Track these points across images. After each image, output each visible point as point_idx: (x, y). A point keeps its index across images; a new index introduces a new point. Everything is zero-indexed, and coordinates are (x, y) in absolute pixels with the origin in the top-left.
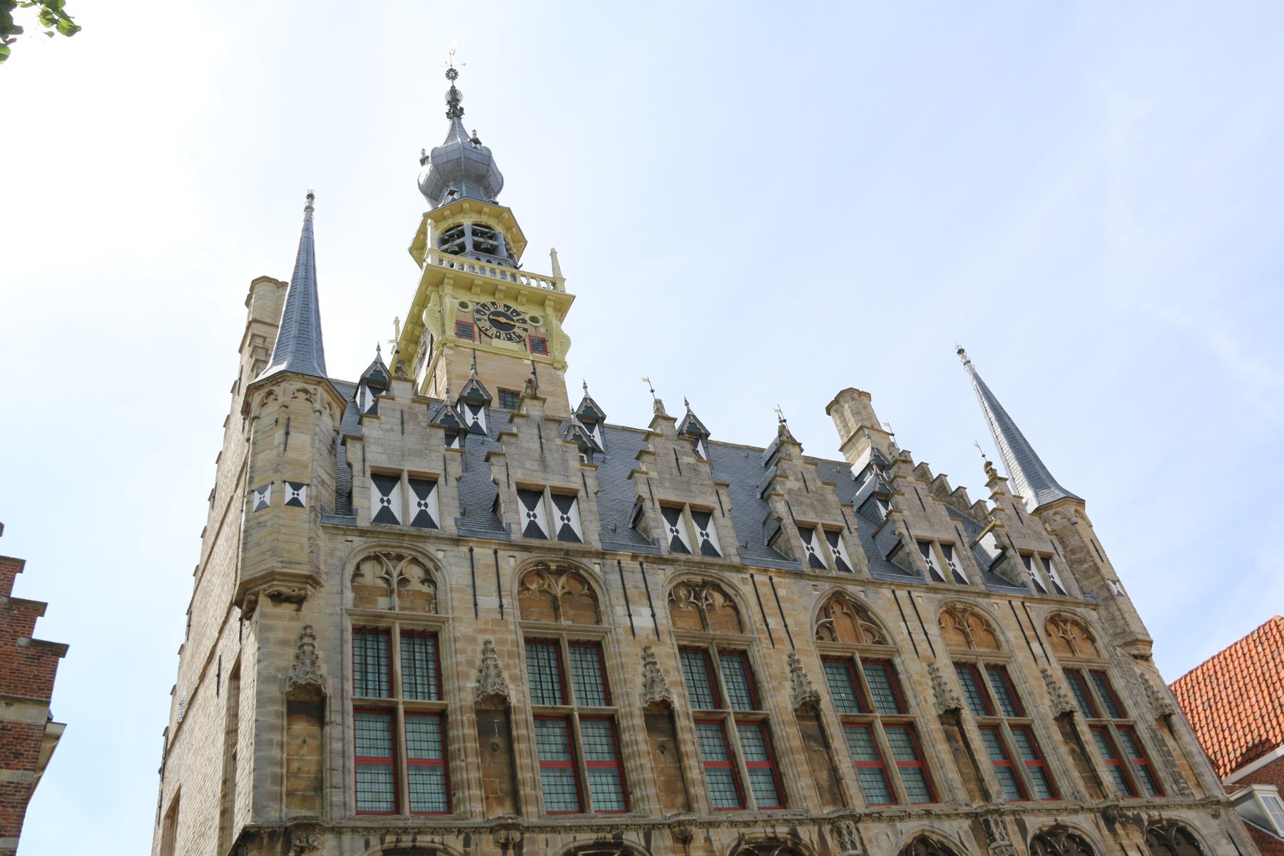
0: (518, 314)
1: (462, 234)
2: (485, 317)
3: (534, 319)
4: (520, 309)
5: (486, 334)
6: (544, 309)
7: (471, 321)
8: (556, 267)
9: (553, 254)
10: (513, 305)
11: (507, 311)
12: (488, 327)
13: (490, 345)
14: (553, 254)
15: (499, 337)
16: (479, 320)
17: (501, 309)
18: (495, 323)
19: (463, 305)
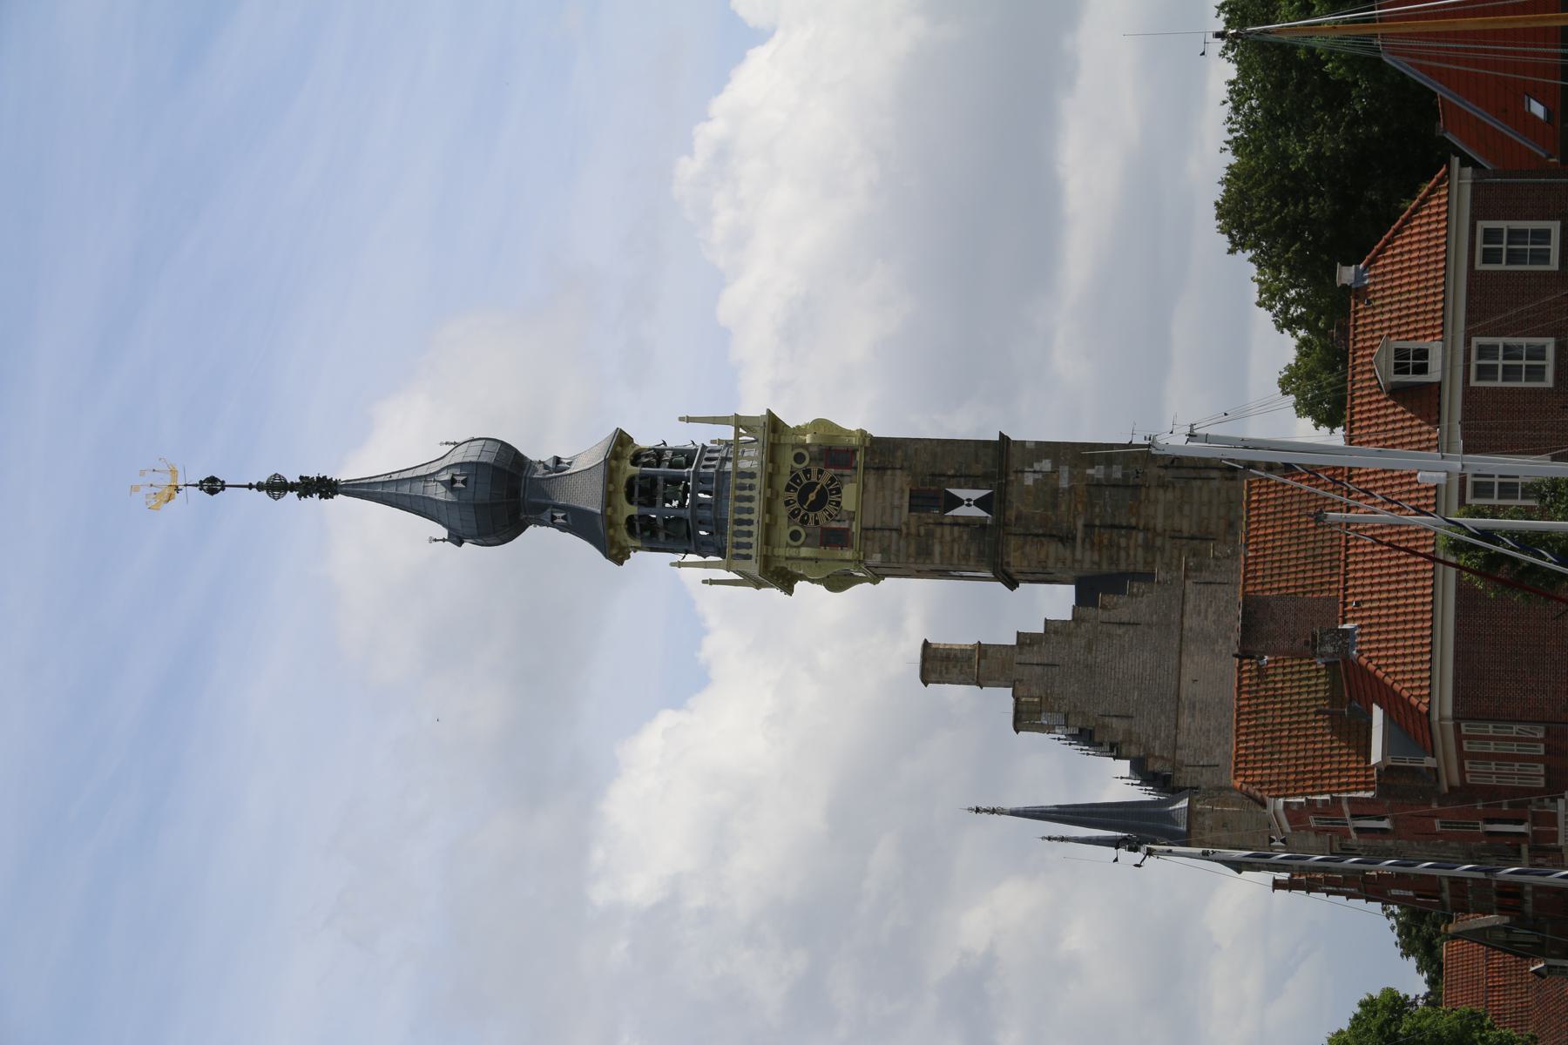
0: (795, 478)
2: (811, 515)
3: (799, 458)
4: (786, 471)
5: (836, 515)
6: (780, 444)
7: (818, 531)
9: (689, 420)
10: (784, 479)
11: (796, 490)
12: (826, 514)
13: (849, 512)
14: (689, 420)
15: (838, 504)
16: (817, 522)
17: (795, 496)
18: (816, 506)
19: (795, 536)
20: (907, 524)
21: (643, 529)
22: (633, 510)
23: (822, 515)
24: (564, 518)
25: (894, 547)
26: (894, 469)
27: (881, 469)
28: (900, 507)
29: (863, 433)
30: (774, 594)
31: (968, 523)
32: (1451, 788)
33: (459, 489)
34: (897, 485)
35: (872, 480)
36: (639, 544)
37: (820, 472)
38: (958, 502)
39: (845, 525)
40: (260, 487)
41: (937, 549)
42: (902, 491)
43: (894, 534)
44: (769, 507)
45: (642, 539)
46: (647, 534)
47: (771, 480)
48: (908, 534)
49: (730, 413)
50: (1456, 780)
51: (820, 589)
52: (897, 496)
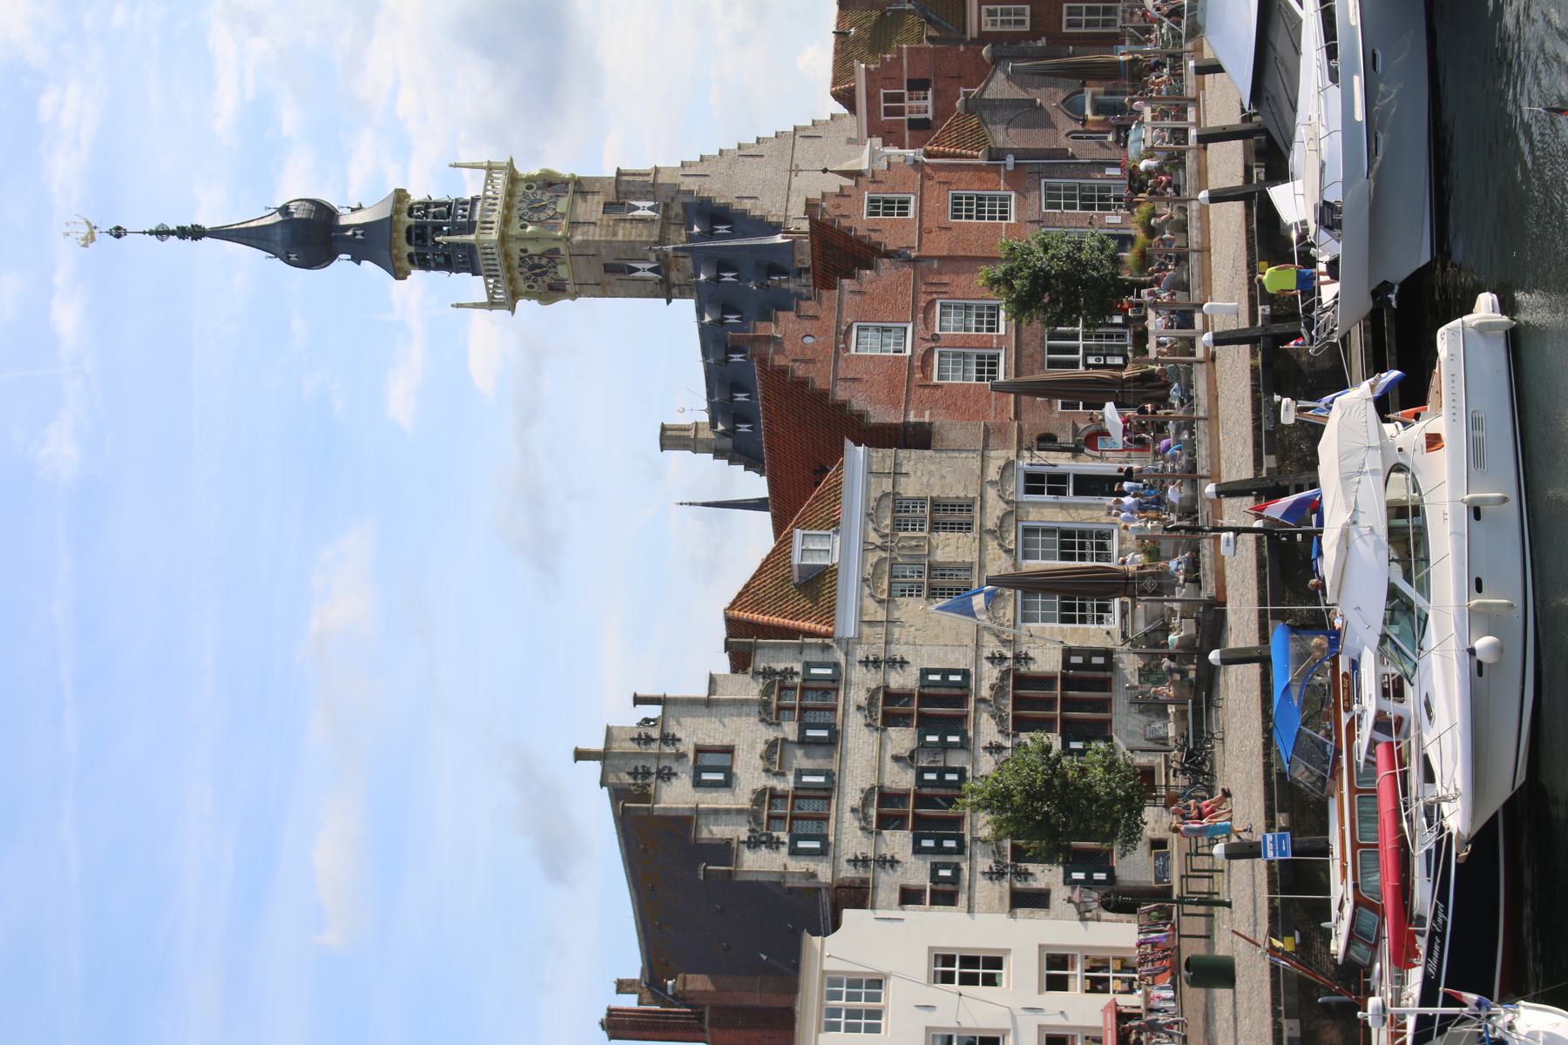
1: (422, 227)
3: (529, 188)
8: (473, 166)
13: (561, 214)
17: (524, 205)
20: (601, 220)
21: (418, 237)
22: (412, 221)
23: (543, 216)
24: (362, 234)
25: (591, 231)
26: (593, 193)
27: (584, 194)
28: (597, 211)
29: (573, 175)
30: (501, 314)
31: (643, 220)
32: (972, 39)
33: (293, 213)
34: (595, 201)
35: (579, 199)
36: (412, 249)
37: (543, 193)
38: (637, 208)
39: (560, 221)
40: (144, 233)
41: (620, 233)
42: (599, 203)
43: (592, 227)
44: (508, 207)
45: (416, 245)
46: (419, 242)
47: (510, 194)
48: (601, 225)
49: (483, 159)
50: (975, 35)
51: (534, 303)
52: (594, 206)
